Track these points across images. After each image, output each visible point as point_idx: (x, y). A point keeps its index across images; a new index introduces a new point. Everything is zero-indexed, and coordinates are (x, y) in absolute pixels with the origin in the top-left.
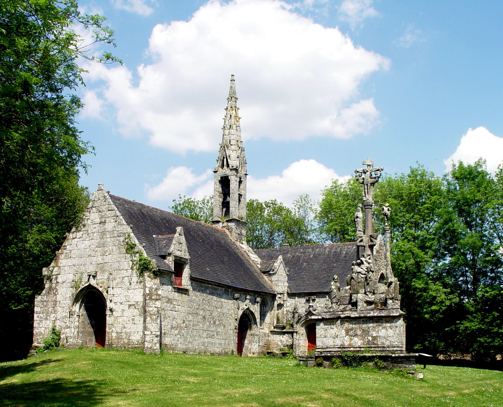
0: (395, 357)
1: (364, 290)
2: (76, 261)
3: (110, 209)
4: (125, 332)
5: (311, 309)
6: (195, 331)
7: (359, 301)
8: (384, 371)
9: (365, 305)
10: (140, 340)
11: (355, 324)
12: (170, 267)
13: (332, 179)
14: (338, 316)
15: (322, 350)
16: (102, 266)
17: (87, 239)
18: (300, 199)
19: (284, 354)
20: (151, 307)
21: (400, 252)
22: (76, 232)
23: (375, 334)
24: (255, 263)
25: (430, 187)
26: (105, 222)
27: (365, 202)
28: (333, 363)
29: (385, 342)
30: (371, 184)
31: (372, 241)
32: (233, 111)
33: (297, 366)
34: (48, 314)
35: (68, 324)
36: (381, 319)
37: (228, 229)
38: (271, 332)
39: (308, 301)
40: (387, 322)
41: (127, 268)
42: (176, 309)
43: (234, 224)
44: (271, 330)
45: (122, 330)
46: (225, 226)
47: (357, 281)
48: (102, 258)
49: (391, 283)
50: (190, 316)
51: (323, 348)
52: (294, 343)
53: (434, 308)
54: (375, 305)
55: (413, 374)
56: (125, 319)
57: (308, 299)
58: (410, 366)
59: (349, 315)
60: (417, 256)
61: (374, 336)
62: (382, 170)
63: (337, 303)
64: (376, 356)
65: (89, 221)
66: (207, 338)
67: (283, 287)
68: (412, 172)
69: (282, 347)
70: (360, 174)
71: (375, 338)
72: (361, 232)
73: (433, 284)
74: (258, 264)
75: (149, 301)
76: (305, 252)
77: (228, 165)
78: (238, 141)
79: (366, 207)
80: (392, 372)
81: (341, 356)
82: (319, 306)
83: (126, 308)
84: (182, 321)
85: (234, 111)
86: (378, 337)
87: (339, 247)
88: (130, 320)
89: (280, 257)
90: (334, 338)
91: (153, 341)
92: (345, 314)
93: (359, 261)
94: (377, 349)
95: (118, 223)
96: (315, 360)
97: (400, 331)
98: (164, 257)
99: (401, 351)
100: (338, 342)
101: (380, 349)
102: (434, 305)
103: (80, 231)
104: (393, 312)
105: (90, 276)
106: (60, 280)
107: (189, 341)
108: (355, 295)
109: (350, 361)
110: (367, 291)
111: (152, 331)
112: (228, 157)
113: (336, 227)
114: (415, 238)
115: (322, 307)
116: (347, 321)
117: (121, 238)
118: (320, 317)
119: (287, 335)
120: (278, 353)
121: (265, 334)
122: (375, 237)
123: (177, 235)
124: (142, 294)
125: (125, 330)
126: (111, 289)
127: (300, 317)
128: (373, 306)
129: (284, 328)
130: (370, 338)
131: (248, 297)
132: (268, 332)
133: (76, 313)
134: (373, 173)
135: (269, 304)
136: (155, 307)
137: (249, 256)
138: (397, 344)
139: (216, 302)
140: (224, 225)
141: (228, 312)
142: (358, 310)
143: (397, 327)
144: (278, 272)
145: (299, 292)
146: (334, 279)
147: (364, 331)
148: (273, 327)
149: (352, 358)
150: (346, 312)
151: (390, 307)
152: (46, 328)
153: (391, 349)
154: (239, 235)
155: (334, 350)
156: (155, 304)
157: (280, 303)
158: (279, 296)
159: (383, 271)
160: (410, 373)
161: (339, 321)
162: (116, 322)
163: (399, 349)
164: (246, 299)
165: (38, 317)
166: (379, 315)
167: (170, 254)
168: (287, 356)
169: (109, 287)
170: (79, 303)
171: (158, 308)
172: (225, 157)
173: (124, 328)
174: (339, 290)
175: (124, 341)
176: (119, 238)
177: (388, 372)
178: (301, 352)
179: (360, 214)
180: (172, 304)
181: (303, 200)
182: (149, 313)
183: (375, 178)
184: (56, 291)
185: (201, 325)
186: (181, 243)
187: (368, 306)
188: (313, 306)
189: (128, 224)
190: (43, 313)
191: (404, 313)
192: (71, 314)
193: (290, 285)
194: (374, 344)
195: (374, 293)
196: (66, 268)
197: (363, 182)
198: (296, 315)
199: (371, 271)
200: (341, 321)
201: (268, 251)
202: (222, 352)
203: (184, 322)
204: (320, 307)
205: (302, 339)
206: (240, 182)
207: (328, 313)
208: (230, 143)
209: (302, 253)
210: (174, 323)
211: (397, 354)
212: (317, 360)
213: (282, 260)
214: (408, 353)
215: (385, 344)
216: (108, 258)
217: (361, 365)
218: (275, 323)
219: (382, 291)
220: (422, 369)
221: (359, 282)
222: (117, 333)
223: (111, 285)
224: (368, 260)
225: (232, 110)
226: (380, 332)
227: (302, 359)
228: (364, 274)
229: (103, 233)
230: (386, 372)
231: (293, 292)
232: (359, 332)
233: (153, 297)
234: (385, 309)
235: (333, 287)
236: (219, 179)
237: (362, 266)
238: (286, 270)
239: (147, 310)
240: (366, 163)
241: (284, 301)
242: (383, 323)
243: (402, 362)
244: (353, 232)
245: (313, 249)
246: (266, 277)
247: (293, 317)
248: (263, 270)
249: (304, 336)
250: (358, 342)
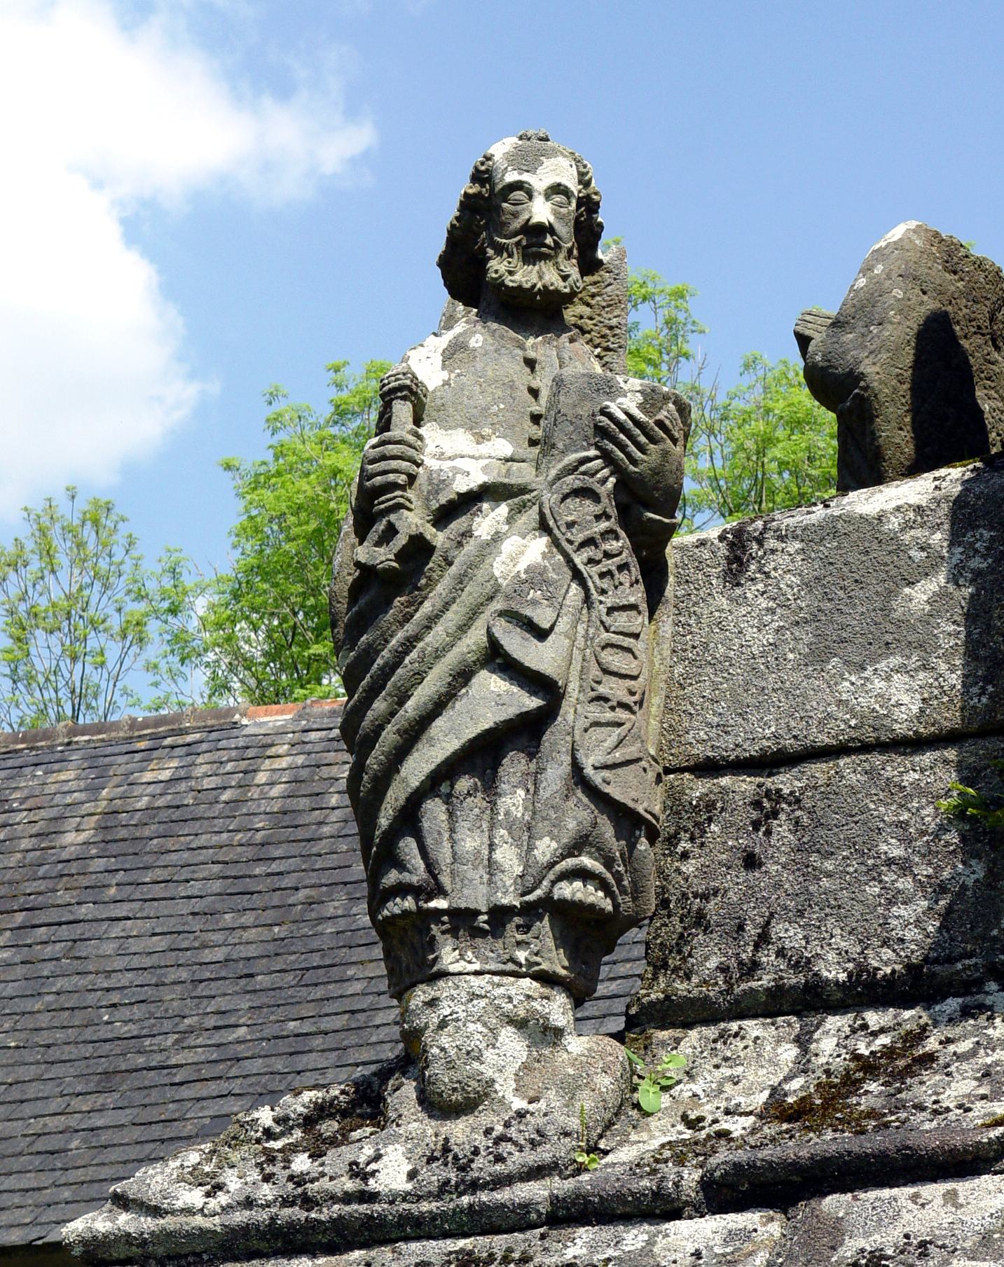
245: (98, 768)
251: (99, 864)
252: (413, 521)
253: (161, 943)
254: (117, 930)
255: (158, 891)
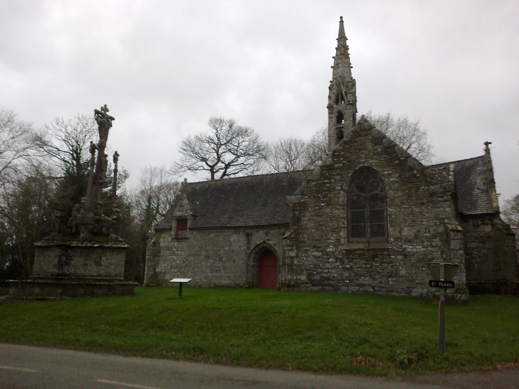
50: (191, 257)
66: (211, 273)
139: (222, 243)
185: (204, 263)
203: (184, 262)
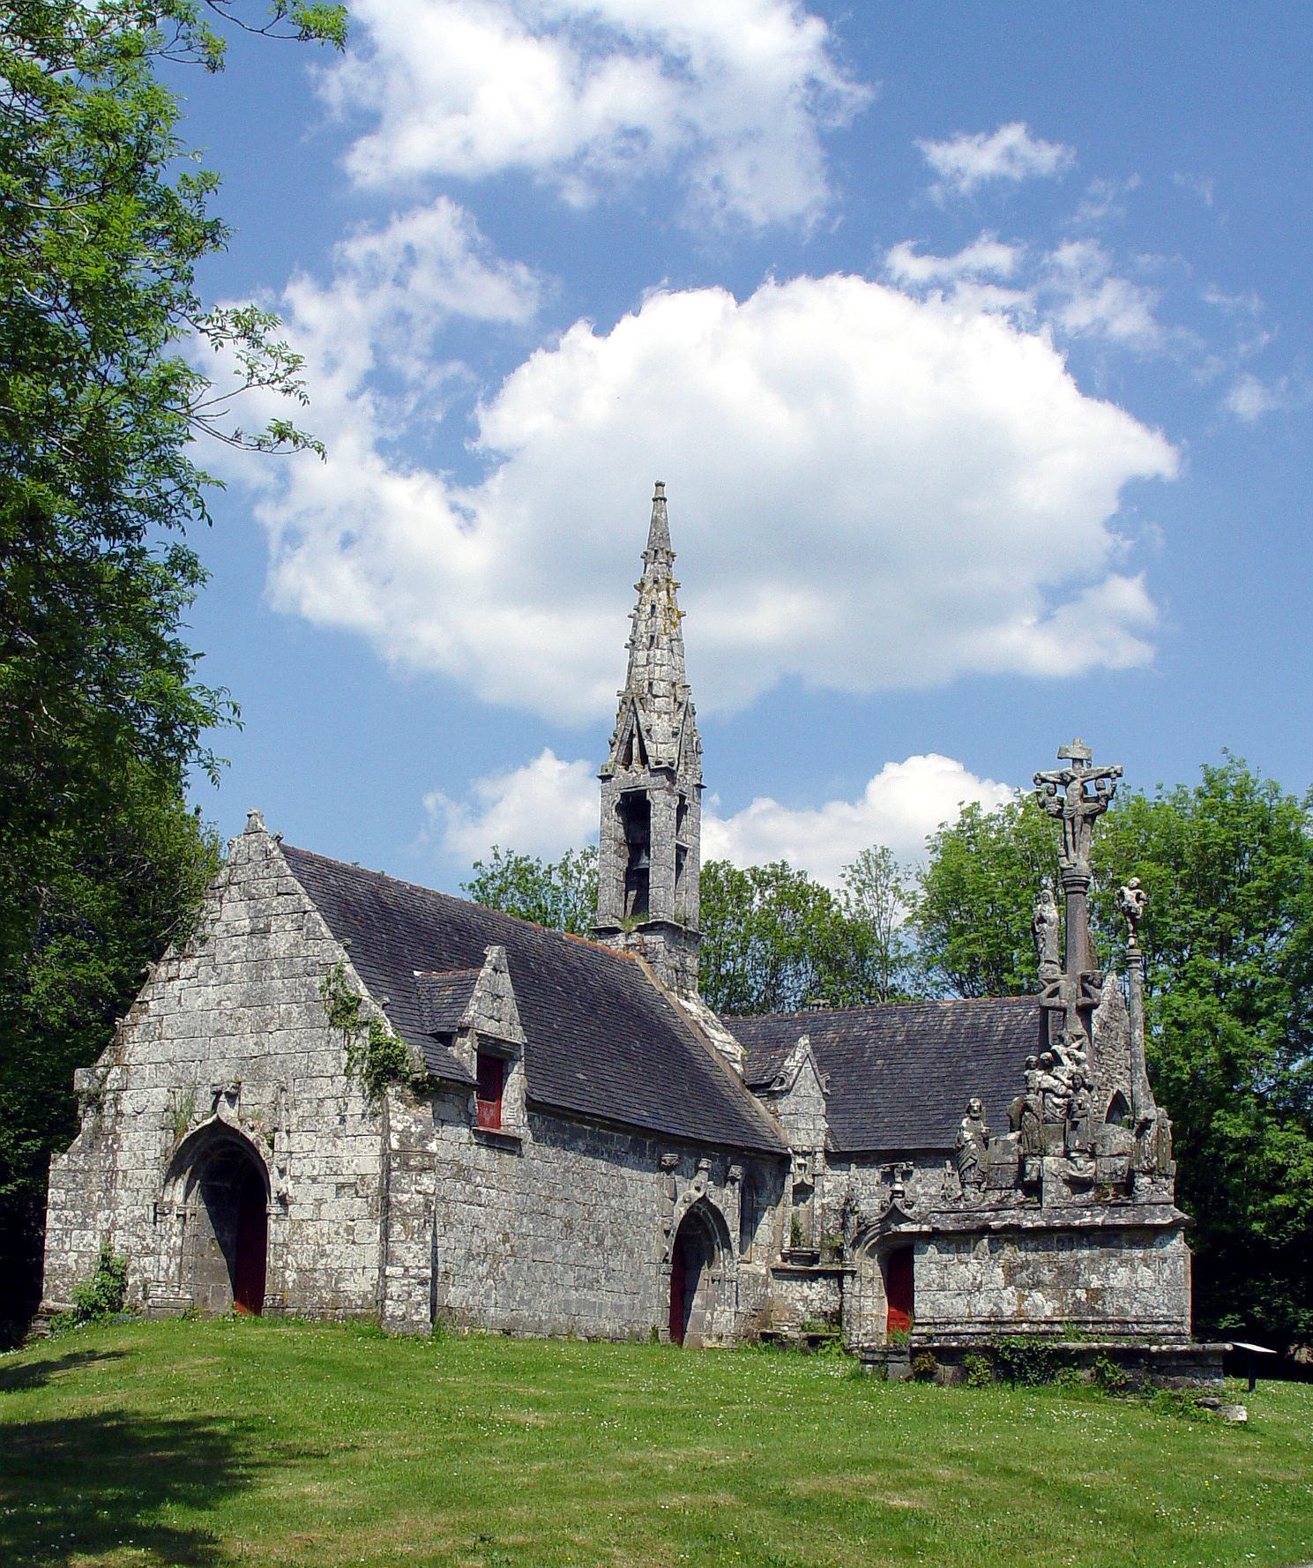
0: (1161, 1354)
1: (1061, 1144)
2: (176, 1049)
3: (282, 889)
4: (325, 1269)
5: (898, 1201)
6: (541, 1266)
7: (1047, 1177)
8: (1125, 1397)
9: (1066, 1190)
10: (370, 1292)
11: (1036, 1250)
12: (463, 1069)
13: (961, 804)
14: (980, 1223)
15: (933, 1330)
16: (255, 1067)
17: (213, 982)
18: (862, 864)
19: (814, 1341)
20: (407, 1193)
21: (1174, 1029)
22: (177, 959)
23: (1096, 1283)
24: (725, 1058)
25: (1264, 828)
26: (267, 930)
27: (1067, 873)
28: (967, 1370)
29: (1127, 1306)
30: (1085, 817)
31: (1086, 993)
32: (660, 594)
33: (854, 1377)
34: (88, 1211)
35: (149, 1240)
36: (1115, 1236)
37: (644, 955)
38: (774, 1270)
39: (888, 1177)
40: (1133, 1244)
41: (332, 1071)
42: (483, 1200)
43: (661, 938)
44: (773, 1265)
45: (316, 1262)
46: (636, 945)
47: (1041, 1117)
48: (255, 1039)
49: (1146, 1124)
51: (936, 1324)
52: (846, 1306)
53: (1279, 1200)
54: (1098, 1191)
55: (1214, 1407)
56: (325, 1227)
57: (888, 1169)
58: (1207, 1383)
59: (1015, 1221)
60: (1230, 1039)
61: (1092, 1286)
62: (1120, 775)
63: (980, 1184)
64: (1100, 1351)
65: (219, 927)
66: (577, 1290)
67: (812, 1134)
68: (1210, 781)
69: (808, 1318)
70: (1052, 786)
71: (1095, 1294)
72: (1053, 965)
73: (1278, 1127)
74: (736, 1061)
75: (398, 1173)
76: (879, 1027)
77: (644, 759)
78: (674, 685)
79: (1068, 890)
80: (1151, 1402)
81: (991, 1348)
82: (922, 1192)
83: (330, 1193)
84: (500, 1236)
85: (663, 594)
86: (1105, 1290)
87: (985, 1010)
88: (341, 1230)
89: (804, 1041)
90: (970, 1293)
91: (410, 1296)
92: (1003, 1219)
93: (1049, 1054)
94: (1103, 1329)
95: (308, 933)
96: (911, 1362)
97: (1173, 1273)
98: (446, 1039)
99: (1179, 1334)
100: (983, 1306)
101: (1111, 1328)
102: (1281, 1191)
103: (189, 956)
104: (1152, 1214)
105: (218, 1094)
106: (127, 1106)
107: (522, 1297)
108: (1036, 1161)
109: (1020, 1366)
110: (1071, 1147)
111: (407, 1264)
112: (644, 734)
113: (975, 949)
114: (1221, 985)
115: (931, 1195)
116: (1011, 1241)
117: (314, 978)
118: (925, 1228)
119: (825, 1283)
120: (797, 1336)
121: (755, 1277)
122: (1095, 982)
123: (486, 970)
124: (378, 1147)
125: (324, 1261)
126: (284, 1134)
127: (863, 1227)
128: (1091, 1193)
129: (814, 1259)
130: (1082, 1294)
131: (704, 1164)
132: (763, 1271)
133: (175, 1208)
134: (1090, 786)
135: (770, 1184)
136: (419, 1193)
137: (707, 1037)
138: (1165, 1312)
139: (605, 1179)
140: (630, 941)
141: (641, 1210)
142: (1044, 1205)
143: (1164, 1260)
144: (796, 1086)
145: (862, 1148)
146: (969, 1111)
147: (1062, 1271)
148: (779, 1257)
149: (1027, 1357)
150: (1006, 1213)
151: (1144, 1199)
152: (81, 1254)
153: (1147, 1328)
154: (677, 971)
155: (970, 1331)
156: (416, 1183)
157: (802, 1181)
158: (800, 1160)
159: (1122, 1086)
160: (1206, 1405)
161: (985, 1241)
162: (296, 1237)
163: (1171, 1329)
164: (698, 1169)
165: (58, 1219)
166: (1109, 1222)
167: (464, 1030)
168: (825, 1346)
169: (276, 1130)
170: (186, 1178)
171: (426, 1194)
172: (635, 731)
173: (323, 1254)
174: (987, 1146)
175: (320, 1297)
176: (309, 979)
177: (1137, 1402)
178: (865, 1335)
179: (1051, 911)
180: (468, 1182)
181: (871, 864)
182: (400, 1210)
183: (1097, 799)
184: (114, 1143)
185: (559, 1249)
186: (499, 997)
187: (1074, 1194)
188: (903, 1192)
189: (338, 938)
190: (73, 1208)
191: (1187, 1217)
192: (160, 1211)
193: (833, 1126)
194: (1093, 1311)
195: (1093, 1156)
196: (147, 1070)
197: (1060, 811)
198: (853, 1219)
199: (1084, 1085)
200: (991, 1242)
201: (765, 1022)
202: (622, 1331)
203: (506, 1239)
204: (924, 1195)
205: (869, 1293)
206: (682, 810)
207: (952, 1215)
208: (650, 691)
209: (871, 1029)
210: (477, 1240)
211: (1165, 1343)
212: (919, 1359)
213: (808, 1048)
214: (1200, 1342)
215: (1128, 1313)
216: (275, 1041)
217: (1053, 1377)
218: (787, 1244)
219: (1120, 1149)
220: (1243, 1391)
221: (1047, 1121)
222: (300, 1270)
223: (284, 1124)
224: (1076, 1052)
225: (657, 590)
226: (1112, 1275)
227: (869, 1357)
228: (1063, 1096)
229: (261, 964)
230: (1131, 1399)
231: (842, 1149)
232: (1047, 1276)
233: (412, 1163)
234: (1128, 1205)
235: (968, 1135)
236: (618, 799)
237: (1057, 1070)
238: (823, 1081)
239: (394, 1200)
240: (1068, 755)
241: (814, 1176)
242: (1121, 1248)
243: (1181, 1371)
244: (1027, 965)
245: (904, 1018)
246: (758, 1103)
247: (843, 1226)
248: (750, 1081)
249: (876, 1285)
250: (1043, 1305)
251: (907, 1046)
252: (963, 1143)
253: (922, 1071)
254: (912, 1066)
255: (921, 1056)
